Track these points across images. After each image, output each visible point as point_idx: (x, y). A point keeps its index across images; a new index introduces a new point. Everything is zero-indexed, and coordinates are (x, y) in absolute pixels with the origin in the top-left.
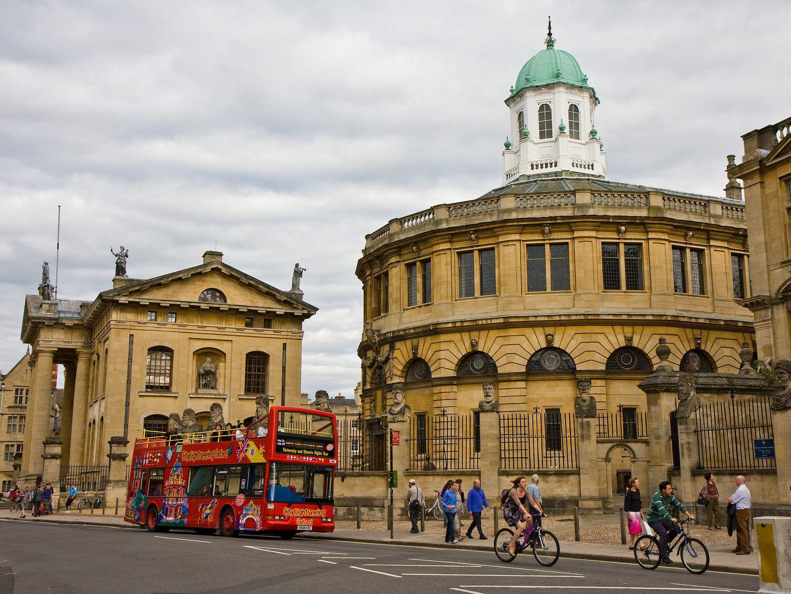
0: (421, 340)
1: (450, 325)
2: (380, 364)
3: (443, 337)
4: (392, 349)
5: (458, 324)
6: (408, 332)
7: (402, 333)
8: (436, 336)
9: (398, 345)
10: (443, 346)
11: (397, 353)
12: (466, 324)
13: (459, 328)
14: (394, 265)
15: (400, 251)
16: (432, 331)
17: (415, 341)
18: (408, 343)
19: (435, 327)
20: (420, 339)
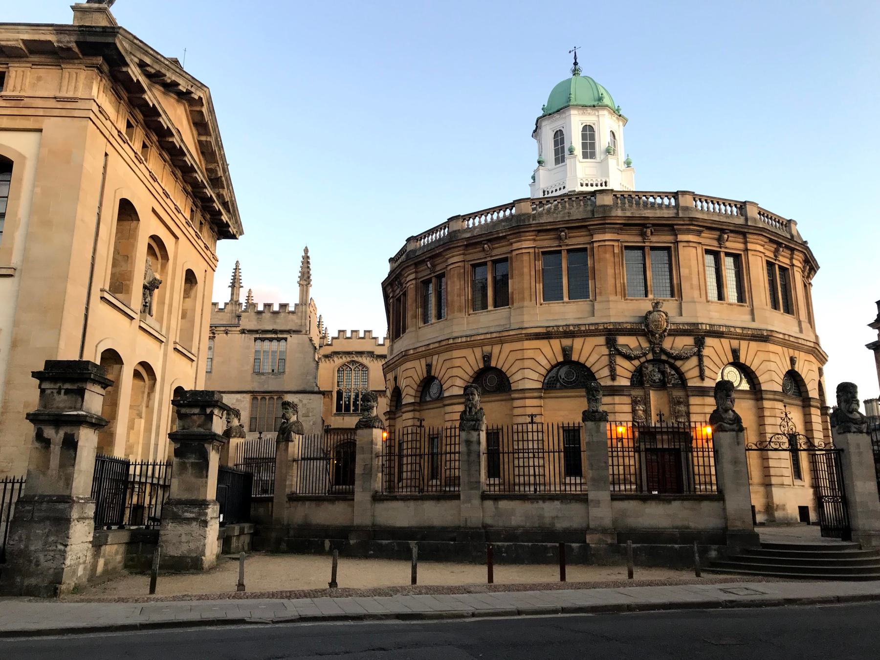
0: (744, 344)
1: (781, 336)
2: (664, 357)
3: (771, 347)
4: (700, 343)
5: (787, 337)
6: (732, 330)
7: (724, 329)
8: (763, 344)
9: (709, 341)
10: (772, 357)
11: (706, 352)
12: (792, 339)
13: (787, 343)
14: (691, 244)
15: (701, 232)
16: (762, 337)
17: (735, 343)
18: (725, 342)
19: (769, 333)
20: (742, 342)
